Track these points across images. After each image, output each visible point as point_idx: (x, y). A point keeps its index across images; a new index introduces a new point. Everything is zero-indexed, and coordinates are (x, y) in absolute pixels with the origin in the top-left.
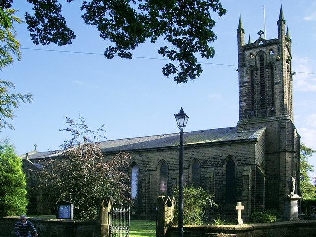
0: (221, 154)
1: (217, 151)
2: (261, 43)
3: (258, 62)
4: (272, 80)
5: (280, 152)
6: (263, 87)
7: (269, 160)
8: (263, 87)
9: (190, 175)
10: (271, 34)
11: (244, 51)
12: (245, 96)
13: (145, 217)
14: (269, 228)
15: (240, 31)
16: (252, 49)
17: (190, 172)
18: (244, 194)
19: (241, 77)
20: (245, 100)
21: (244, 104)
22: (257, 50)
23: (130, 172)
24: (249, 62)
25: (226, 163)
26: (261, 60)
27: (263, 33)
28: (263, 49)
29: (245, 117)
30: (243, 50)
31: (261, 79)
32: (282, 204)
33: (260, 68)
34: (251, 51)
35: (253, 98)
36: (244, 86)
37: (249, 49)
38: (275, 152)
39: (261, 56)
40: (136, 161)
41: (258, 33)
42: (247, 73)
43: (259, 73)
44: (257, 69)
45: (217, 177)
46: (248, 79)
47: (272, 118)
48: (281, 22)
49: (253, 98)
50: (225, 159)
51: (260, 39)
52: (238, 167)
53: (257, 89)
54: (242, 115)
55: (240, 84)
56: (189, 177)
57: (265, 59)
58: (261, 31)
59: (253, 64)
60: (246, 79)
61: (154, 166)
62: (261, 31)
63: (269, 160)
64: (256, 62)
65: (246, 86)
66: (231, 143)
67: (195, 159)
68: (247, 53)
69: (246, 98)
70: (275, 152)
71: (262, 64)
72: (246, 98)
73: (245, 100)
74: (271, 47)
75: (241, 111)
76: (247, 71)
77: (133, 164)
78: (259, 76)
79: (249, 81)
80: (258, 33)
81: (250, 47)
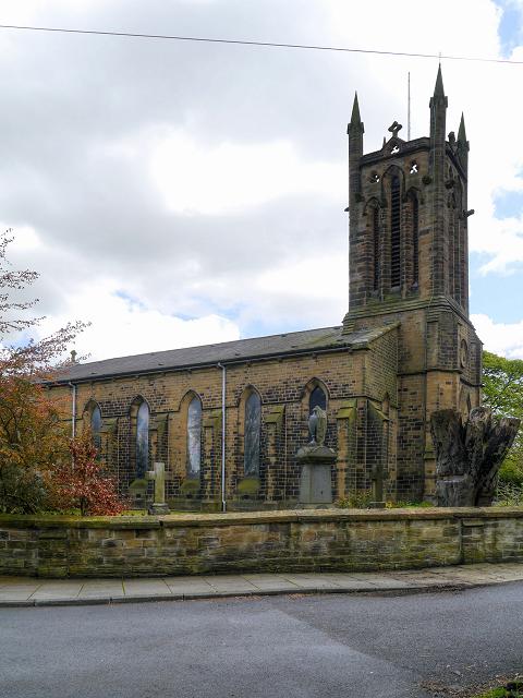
0: (298, 376)
1: (290, 370)
2: (396, 151)
3: (388, 191)
4: (416, 227)
5: (424, 373)
6: (396, 239)
7: (406, 390)
8: (396, 239)
9: (240, 421)
10: (418, 127)
11: (360, 168)
12: (360, 261)
13: (273, 505)
14: (281, 523)
15: (356, 129)
16: (376, 162)
17: (242, 414)
18: (340, 458)
19: (353, 223)
20: (360, 269)
21: (358, 276)
22: (385, 165)
23: (134, 414)
24: (370, 191)
25: (308, 395)
26: (394, 186)
27: (400, 127)
28: (400, 163)
29: (360, 303)
30: (360, 163)
31: (393, 225)
32: (429, 480)
33: (393, 202)
34: (374, 168)
35: (376, 264)
36: (358, 242)
37: (370, 164)
38: (417, 374)
39: (393, 176)
40: (144, 394)
41: (390, 130)
42: (364, 214)
43: (389, 213)
44: (384, 206)
45: (290, 423)
46: (368, 226)
47: (412, 304)
48: (439, 103)
49: (376, 264)
50: (306, 386)
51: (395, 142)
52: (330, 402)
53: (384, 245)
54: (354, 301)
55: (351, 236)
56: (239, 424)
57: (401, 182)
58: (395, 124)
59: (378, 194)
60: (362, 227)
61: (176, 403)
62: (395, 124)
63: (406, 390)
64: (383, 190)
65: (362, 241)
66: (318, 354)
67: (250, 387)
68: (366, 172)
69: (361, 265)
70: (417, 374)
71: (395, 195)
72: (361, 265)
73: (360, 269)
74: (413, 157)
75: (351, 291)
76: (365, 210)
77: (139, 400)
78: (389, 220)
79: (371, 229)
80: (390, 130)
81: (375, 158)
